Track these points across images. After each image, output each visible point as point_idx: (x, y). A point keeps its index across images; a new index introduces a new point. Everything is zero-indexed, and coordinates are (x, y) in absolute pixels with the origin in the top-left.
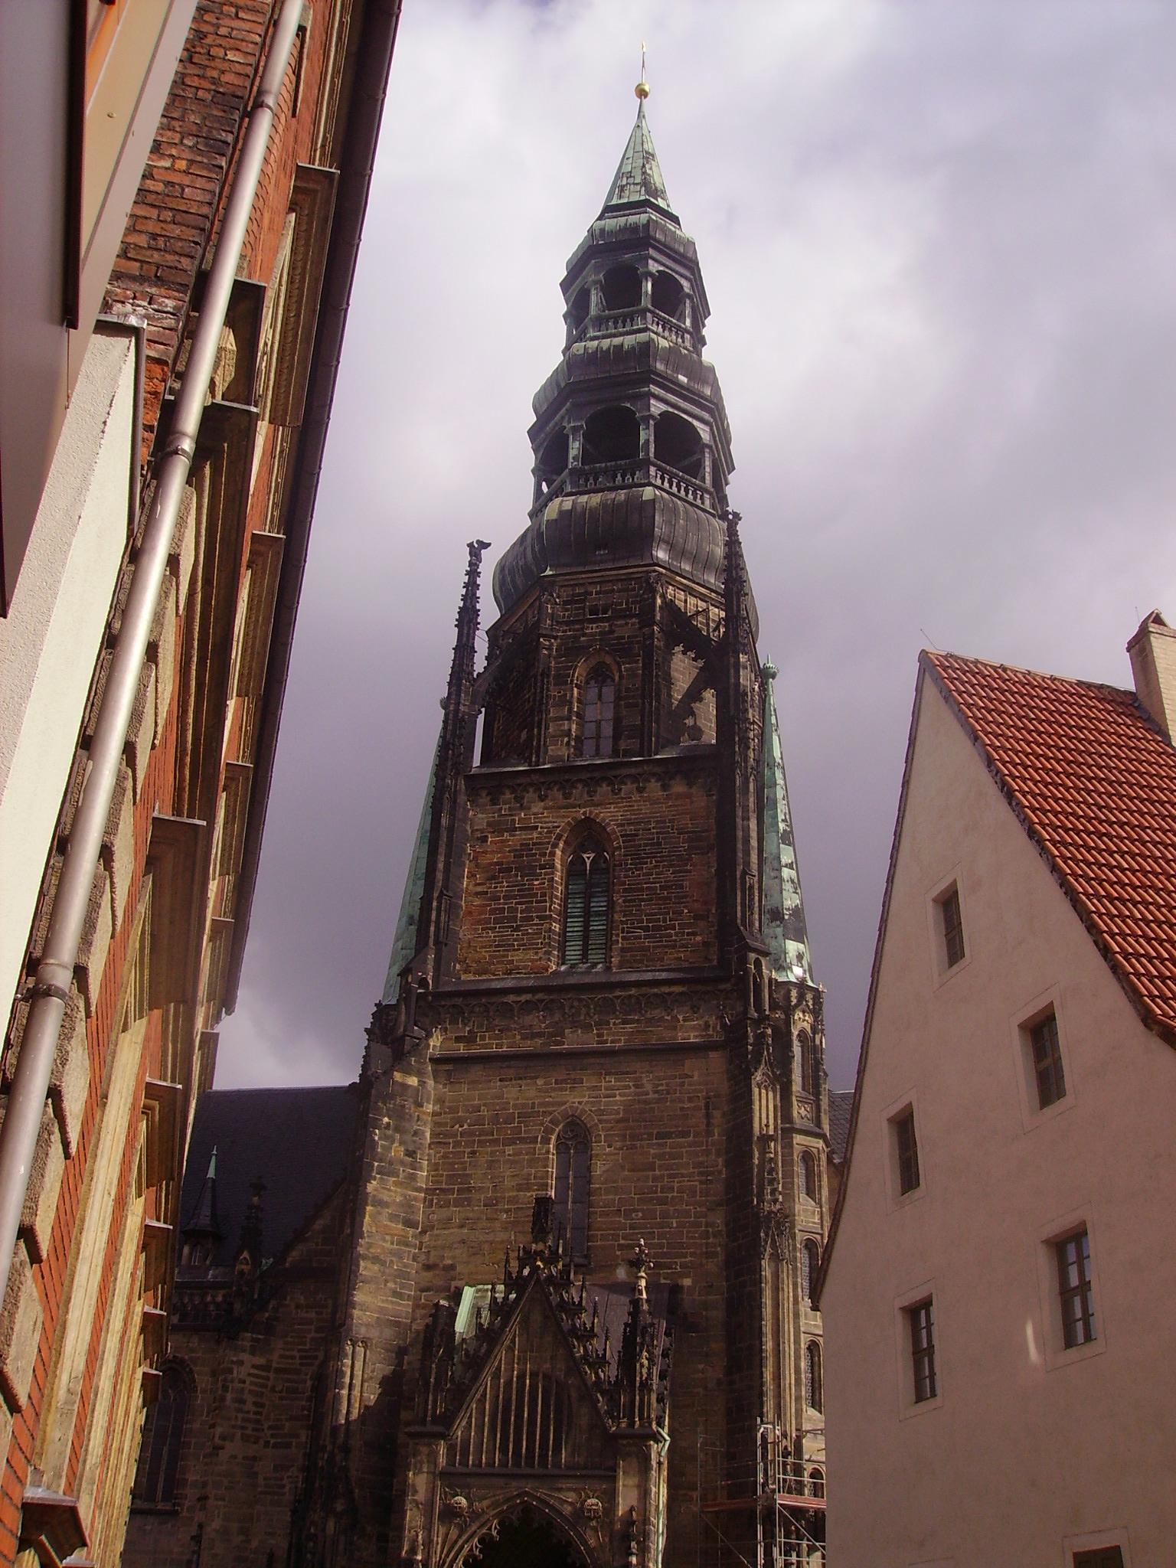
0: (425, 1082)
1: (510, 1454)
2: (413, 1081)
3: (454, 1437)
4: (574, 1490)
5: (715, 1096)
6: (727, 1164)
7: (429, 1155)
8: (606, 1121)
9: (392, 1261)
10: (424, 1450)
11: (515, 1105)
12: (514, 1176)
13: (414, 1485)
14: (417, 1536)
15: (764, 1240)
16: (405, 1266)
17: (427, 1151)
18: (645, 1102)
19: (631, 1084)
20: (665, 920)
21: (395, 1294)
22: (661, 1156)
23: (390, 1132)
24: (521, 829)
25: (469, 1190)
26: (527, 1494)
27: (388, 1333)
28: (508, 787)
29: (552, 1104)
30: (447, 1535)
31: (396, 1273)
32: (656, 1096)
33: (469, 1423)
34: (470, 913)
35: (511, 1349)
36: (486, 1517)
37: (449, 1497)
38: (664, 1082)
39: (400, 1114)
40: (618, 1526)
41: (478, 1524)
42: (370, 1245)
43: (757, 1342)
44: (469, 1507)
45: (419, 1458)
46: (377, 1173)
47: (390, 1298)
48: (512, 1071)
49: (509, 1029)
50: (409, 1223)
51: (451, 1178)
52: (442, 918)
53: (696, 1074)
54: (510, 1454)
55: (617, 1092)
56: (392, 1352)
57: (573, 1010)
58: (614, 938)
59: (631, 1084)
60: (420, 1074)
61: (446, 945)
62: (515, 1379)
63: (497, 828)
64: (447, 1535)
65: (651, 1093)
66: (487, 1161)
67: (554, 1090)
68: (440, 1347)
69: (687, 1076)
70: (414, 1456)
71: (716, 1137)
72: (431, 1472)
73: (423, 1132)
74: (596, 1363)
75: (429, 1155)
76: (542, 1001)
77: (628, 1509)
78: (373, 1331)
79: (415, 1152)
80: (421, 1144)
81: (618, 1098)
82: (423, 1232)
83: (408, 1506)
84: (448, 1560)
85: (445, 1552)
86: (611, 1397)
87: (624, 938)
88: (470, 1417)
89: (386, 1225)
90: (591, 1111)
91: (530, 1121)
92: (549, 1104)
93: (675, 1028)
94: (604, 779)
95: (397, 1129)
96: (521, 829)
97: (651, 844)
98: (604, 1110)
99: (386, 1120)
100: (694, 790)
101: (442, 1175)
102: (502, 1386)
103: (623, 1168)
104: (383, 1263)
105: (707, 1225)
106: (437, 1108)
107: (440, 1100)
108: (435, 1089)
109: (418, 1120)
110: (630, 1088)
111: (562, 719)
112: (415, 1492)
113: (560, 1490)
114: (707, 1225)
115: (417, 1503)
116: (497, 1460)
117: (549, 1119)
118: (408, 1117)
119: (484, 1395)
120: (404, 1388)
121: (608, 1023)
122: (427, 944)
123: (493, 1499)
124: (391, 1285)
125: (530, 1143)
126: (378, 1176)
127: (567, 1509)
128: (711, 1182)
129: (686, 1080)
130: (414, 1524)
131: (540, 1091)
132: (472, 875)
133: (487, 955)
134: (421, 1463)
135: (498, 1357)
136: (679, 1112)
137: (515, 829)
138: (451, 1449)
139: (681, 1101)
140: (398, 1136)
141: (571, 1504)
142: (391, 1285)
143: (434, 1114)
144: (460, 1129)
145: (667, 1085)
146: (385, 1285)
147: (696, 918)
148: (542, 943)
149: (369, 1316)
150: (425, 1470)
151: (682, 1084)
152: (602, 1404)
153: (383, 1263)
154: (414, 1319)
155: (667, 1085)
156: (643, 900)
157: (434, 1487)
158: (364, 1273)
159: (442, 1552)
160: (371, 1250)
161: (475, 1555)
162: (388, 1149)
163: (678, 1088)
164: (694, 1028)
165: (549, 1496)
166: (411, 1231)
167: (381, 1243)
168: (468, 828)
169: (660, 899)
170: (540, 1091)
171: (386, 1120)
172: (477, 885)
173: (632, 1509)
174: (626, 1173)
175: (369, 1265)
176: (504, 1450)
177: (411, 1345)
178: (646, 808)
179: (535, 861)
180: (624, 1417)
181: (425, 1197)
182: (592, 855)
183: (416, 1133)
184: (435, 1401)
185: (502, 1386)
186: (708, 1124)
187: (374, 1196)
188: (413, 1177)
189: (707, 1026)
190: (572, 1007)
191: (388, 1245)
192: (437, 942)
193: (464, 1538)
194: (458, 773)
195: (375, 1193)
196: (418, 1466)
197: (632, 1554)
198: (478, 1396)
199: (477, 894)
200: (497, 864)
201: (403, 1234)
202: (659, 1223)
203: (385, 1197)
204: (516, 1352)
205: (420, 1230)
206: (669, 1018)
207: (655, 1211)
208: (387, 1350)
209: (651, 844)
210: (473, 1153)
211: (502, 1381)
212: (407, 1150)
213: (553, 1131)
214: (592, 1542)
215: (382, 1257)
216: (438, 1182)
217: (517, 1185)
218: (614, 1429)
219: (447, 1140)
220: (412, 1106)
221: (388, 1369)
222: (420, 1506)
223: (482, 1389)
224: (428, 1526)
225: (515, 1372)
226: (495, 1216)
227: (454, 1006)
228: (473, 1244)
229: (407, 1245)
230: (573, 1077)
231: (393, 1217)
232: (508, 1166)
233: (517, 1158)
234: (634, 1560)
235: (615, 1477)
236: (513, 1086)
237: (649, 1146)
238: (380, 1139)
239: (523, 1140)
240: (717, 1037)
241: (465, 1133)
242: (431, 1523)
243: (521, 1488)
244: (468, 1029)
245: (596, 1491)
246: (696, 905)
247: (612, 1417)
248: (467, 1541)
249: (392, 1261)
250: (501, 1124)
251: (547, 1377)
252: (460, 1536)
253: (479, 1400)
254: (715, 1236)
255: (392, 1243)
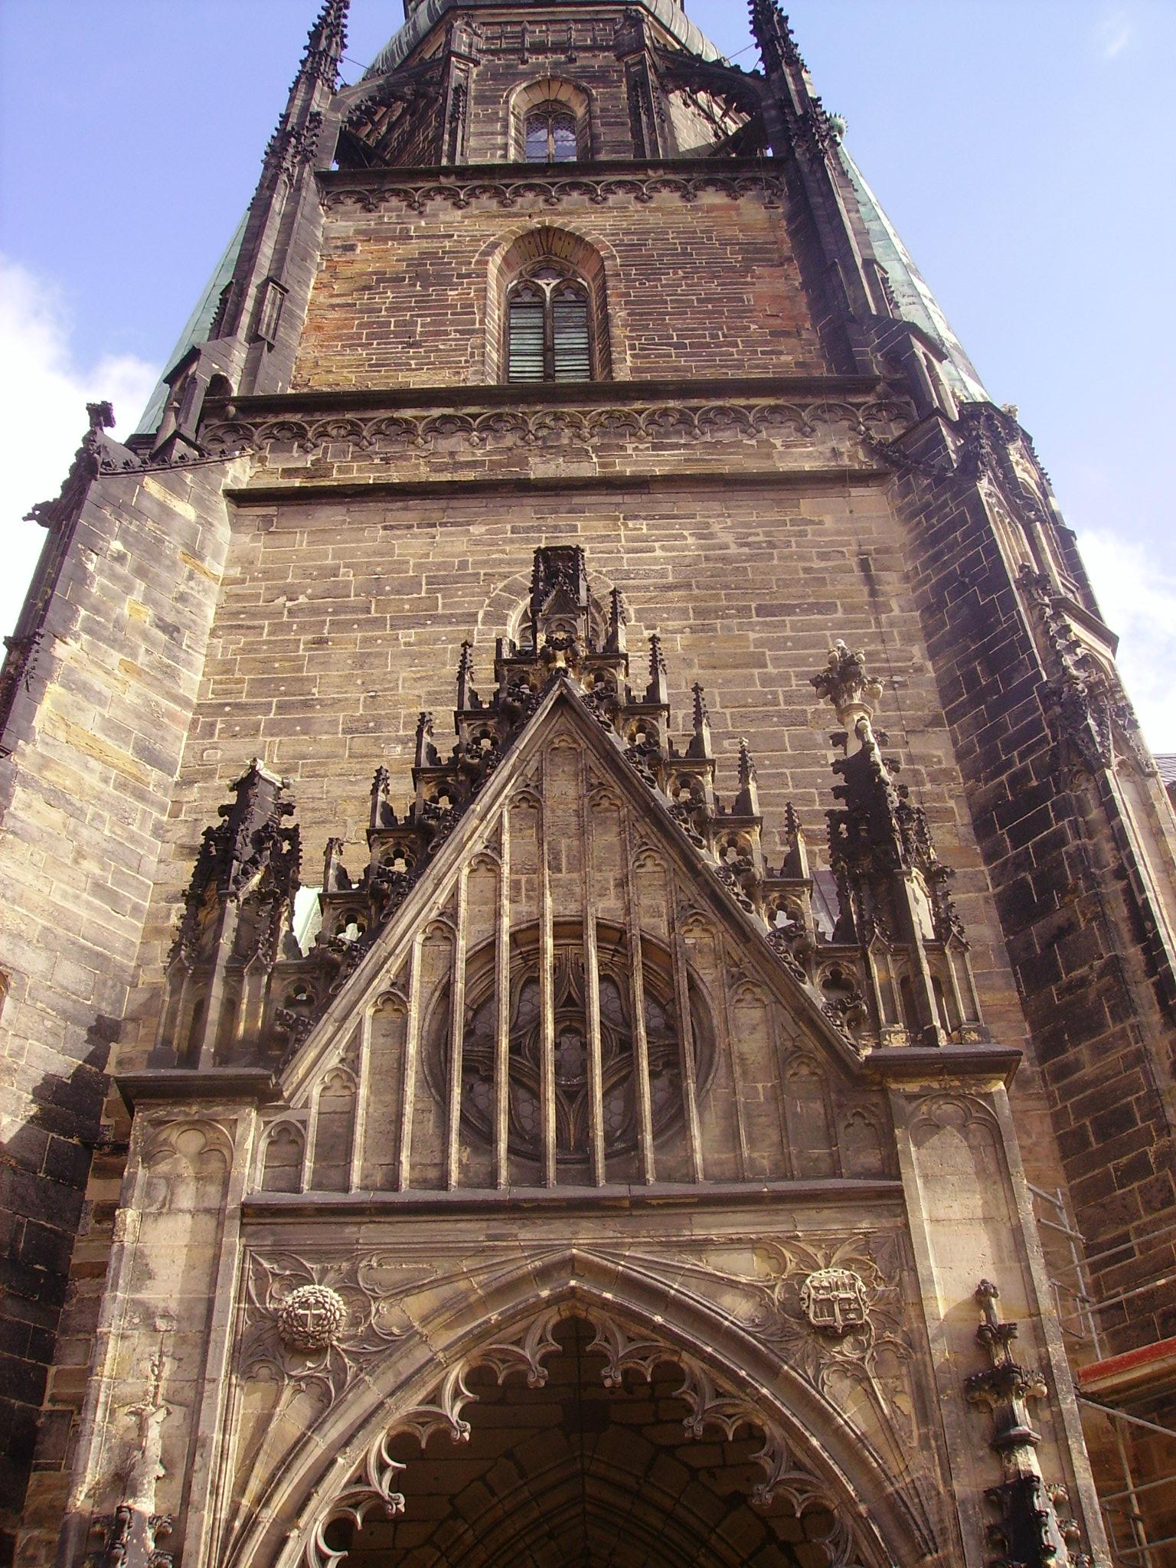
0: (211, 525)
1: (503, 1146)
2: (186, 510)
3: (297, 1102)
4: (754, 1245)
5: (878, 551)
6: (933, 653)
7: (209, 646)
8: (638, 588)
9: (97, 817)
10: (189, 1142)
11: (418, 566)
12: (415, 680)
13: (138, 1255)
14: (142, 1428)
15: (1102, 735)
16: (132, 838)
17: (206, 639)
18: (723, 559)
19: (686, 533)
20: (714, 336)
21: (99, 888)
22: (778, 644)
23: (124, 570)
24: (418, 237)
25: (307, 705)
26: (572, 1265)
27: (72, 974)
28: (397, 193)
29: (509, 563)
30: (263, 1423)
31: (109, 846)
32: (746, 550)
33: (351, 1062)
34: (319, 328)
35: (488, 861)
36: (421, 1355)
37: (275, 1287)
38: (759, 530)
39: (153, 549)
40: (941, 1353)
41: (389, 1380)
42: (45, 763)
43: (1134, 953)
44: (355, 1322)
45: (163, 1167)
46: (89, 631)
47: (85, 896)
48: (410, 515)
49: (408, 458)
50: (148, 755)
51: (261, 686)
52: (267, 308)
53: (829, 521)
54: (503, 1146)
55: (657, 545)
56: (75, 1020)
57: (544, 432)
58: (614, 356)
59: (686, 533)
60: (200, 503)
61: (271, 347)
62: (505, 938)
63: (368, 236)
64: (263, 1423)
65: (733, 546)
66: (353, 655)
67: (512, 541)
68: (254, 862)
69: (812, 522)
70: (149, 1159)
71: (896, 612)
72: (208, 1211)
73: (199, 605)
74: (768, 886)
75: (209, 646)
76: (475, 417)
77: (966, 1294)
78: (30, 954)
79: (178, 630)
80: (194, 621)
81: (658, 553)
82: (187, 782)
83: (113, 1322)
84: (268, 1515)
85: (254, 1486)
86: (836, 975)
87: (633, 356)
88: (355, 1043)
89: (94, 738)
90: (600, 573)
91: (458, 589)
92: (501, 562)
93: (769, 456)
94: (575, 186)
95: (141, 572)
96: (418, 237)
97: (673, 255)
98: (628, 572)
99: (117, 545)
100: (741, 201)
101: (242, 681)
102: (461, 957)
103: (689, 665)
104: (76, 813)
105: (911, 759)
106: (236, 572)
107: (245, 561)
108: (232, 543)
109: (191, 577)
110: (685, 538)
111: (492, 134)
112: (144, 1274)
113: (699, 1247)
114: (911, 759)
115: (148, 1315)
116: (454, 1167)
117: (501, 585)
118: (168, 562)
119: (402, 982)
120: (103, 1121)
121: (622, 448)
122: (232, 331)
123: (446, 1291)
124: (90, 866)
125: (458, 623)
126: (85, 637)
127: (737, 1310)
128: (903, 685)
129: (809, 528)
130: (131, 1387)
131: (477, 543)
132: (320, 286)
133: (353, 377)
134: (172, 1181)
135: (448, 882)
136: (802, 575)
137: (411, 238)
138: (287, 1138)
139: (802, 558)
140: (140, 585)
141: (750, 1291)
142: (90, 866)
143: (227, 582)
144: (289, 604)
145: (767, 534)
146: (76, 861)
147: (772, 334)
148: (466, 361)
149: (22, 917)
150: (186, 1197)
151: (802, 534)
152: (813, 989)
153: (76, 813)
154: (143, 962)
155: (767, 534)
156: (668, 314)
157: (216, 1258)
158: (21, 814)
159: (241, 1488)
160: (47, 774)
161: (377, 1495)
162: (118, 599)
163: (793, 539)
164: (809, 455)
165: (665, 1269)
166: (155, 775)
167: (75, 768)
168: (319, 234)
169: (699, 312)
170: (477, 543)
171: (117, 545)
172: (332, 296)
173: (983, 1295)
174: (696, 670)
175: (39, 804)
176: (479, 1132)
177: (133, 1019)
178: (654, 220)
179: (453, 269)
180: (893, 1020)
181: (195, 722)
182: (554, 283)
183: (182, 598)
184: (231, 1006)
185: (461, 957)
186: (873, 593)
187: (71, 670)
188: (171, 674)
189: (836, 453)
190: (541, 426)
191: (92, 780)
192: (254, 338)
193: (335, 1430)
194: (305, 160)
195: (73, 664)
196: (162, 1191)
197: (1024, 1440)
198: (382, 984)
199: (333, 307)
200: (375, 273)
201: (134, 771)
202: (793, 756)
203: (98, 681)
204: (506, 870)
205: (176, 778)
206: (753, 442)
207: (777, 737)
208: (66, 1016)
209: (673, 255)
210: (321, 642)
211: (462, 944)
212: (160, 619)
213: (511, 604)
214: (853, 1416)
215: (75, 799)
216: (227, 692)
217: (429, 693)
218: (867, 1052)
219: (256, 623)
220: (181, 549)
221: (64, 1065)
222: (161, 1324)
223: (394, 965)
224: (189, 1394)
225: (506, 922)
226: (377, 751)
227: (282, 426)
228: (315, 805)
229: (141, 796)
230: (550, 522)
231: (112, 728)
232: (407, 661)
233: (425, 648)
234: (1029, 1461)
235: (899, 1193)
236: (414, 536)
237: (751, 626)
238: (101, 571)
239: (436, 619)
240: (859, 460)
241: (302, 610)
242: (200, 1379)
243: (551, 1248)
244: (311, 458)
245: (834, 1244)
246: (772, 321)
247: (856, 1022)
248: (347, 1441)
249: (97, 817)
250: (388, 594)
251: (613, 937)
252: (316, 1424)
253: (388, 998)
254: (933, 781)
255: (106, 781)
